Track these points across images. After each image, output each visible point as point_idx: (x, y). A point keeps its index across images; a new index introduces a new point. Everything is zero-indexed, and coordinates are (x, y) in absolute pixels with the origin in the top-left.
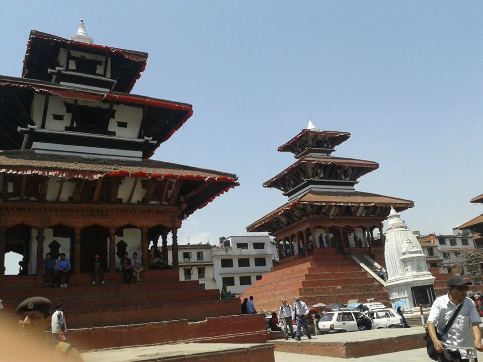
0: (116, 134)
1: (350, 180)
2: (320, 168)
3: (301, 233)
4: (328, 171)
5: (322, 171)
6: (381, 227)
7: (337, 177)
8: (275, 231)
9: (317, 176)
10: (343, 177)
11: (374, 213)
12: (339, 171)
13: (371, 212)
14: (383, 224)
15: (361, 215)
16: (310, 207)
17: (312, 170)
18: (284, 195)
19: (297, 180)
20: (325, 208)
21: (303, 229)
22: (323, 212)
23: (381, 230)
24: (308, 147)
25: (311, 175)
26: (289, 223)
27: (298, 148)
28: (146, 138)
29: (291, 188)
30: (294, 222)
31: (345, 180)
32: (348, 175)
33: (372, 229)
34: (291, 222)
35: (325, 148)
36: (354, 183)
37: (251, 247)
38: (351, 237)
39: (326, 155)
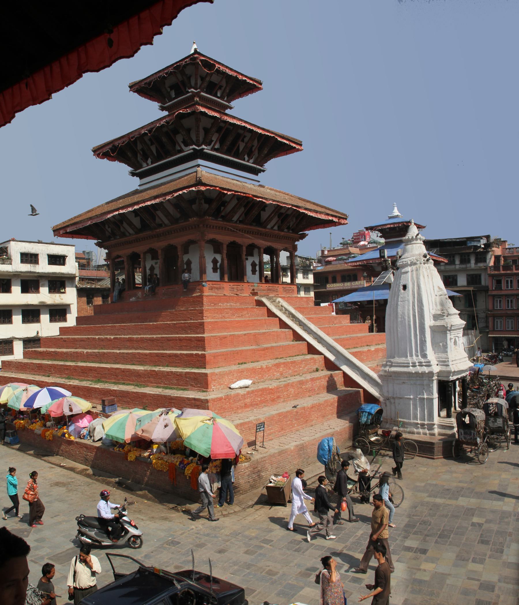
4: (230, 139)
9: (209, 145)
15: (272, 228)
18: (133, 174)
26: (145, 226)
27: (169, 90)
29: (149, 161)
30: (160, 226)
35: (218, 98)
36: (260, 171)
37: (43, 260)
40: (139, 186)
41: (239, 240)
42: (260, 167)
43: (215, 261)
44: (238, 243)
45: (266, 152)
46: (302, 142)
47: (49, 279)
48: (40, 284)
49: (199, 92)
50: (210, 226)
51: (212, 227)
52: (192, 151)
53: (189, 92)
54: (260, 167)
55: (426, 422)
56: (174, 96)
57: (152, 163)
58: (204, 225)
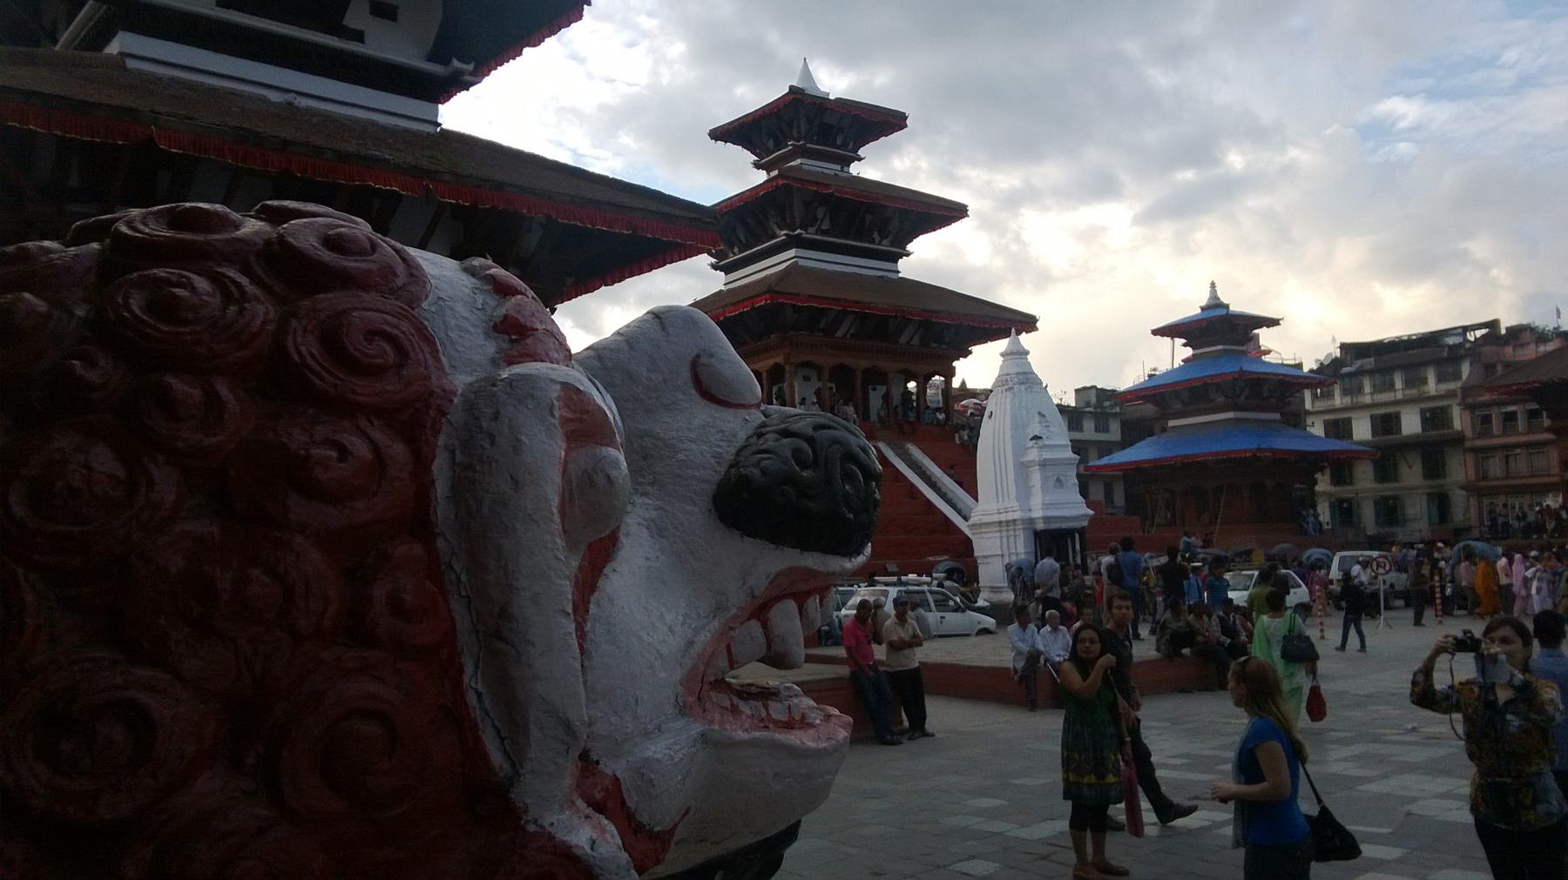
0: (367, 39)
6: (949, 373)
9: (812, 226)
10: (876, 235)
12: (869, 218)
14: (954, 368)
15: (908, 342)
18: (715, 267)
24: (795, 140)
25: (798, 224)
28: (456, 63)
29: (736, 250)
31: (880, 244)
32: (889, 232)
35: (838, 147)
39: (839, 167)
40: (725, 284)
41: (850, 361)
42: (900, 251)
52: (784, 237)
53: (788, 146)
54: (900, 251)
56: (772, 149)
57: (740, 253)
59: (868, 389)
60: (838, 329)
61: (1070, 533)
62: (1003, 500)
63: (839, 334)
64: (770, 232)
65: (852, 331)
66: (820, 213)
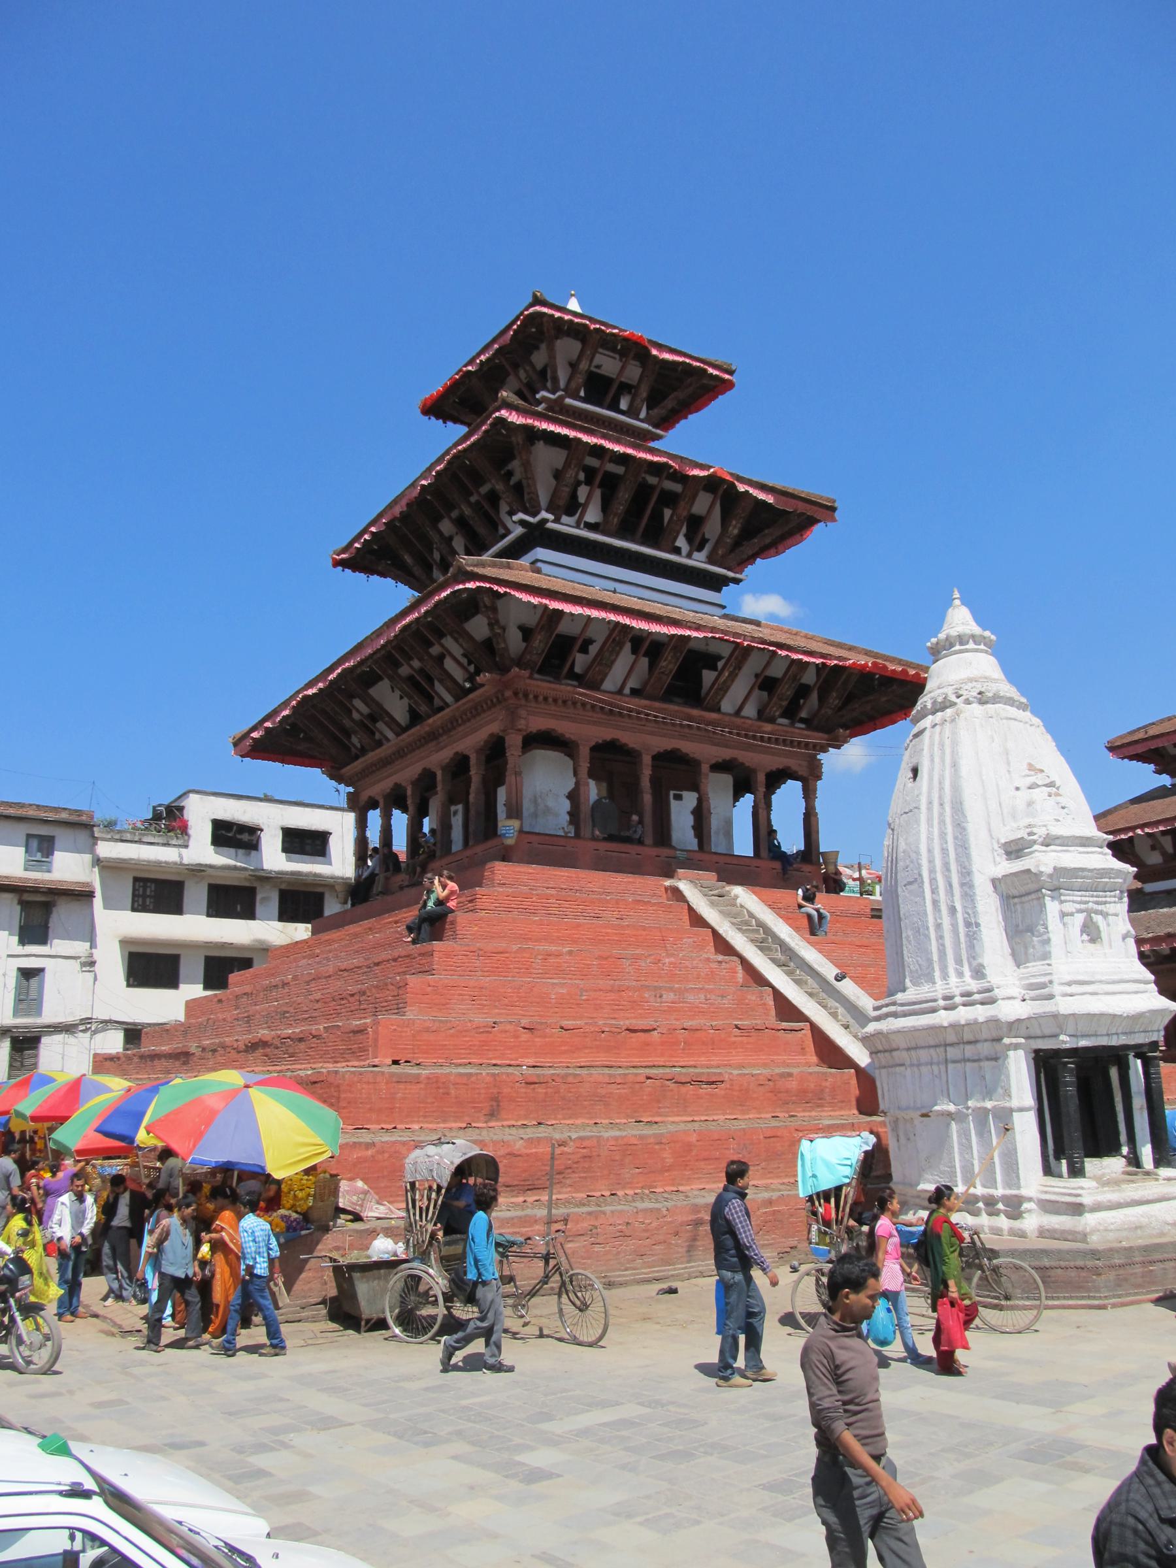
1: (711, 560)
2: (589, 481)
3: (460, 766)
4: (624, 495)
5: (598, 493)
6: (810, 777)
7: (656, 535)
8: (357, 758)
9: (570, 514)
11: (790, 713)
12: (667, 513)
13: (785, 703)
15: (738, 713)
16: (520, 635)
17: (554, 482)
19: (482, 530)
20: (584, 649)
21: (470, 741)
22: (578, 669)
23: (809, 794)
25: (544, 500)
26: (415, 718)
33: (776, 779)
34: (423, 709)
36: (726, 581)
38: (681, 812)
41: (629, 739)
43: (573, 796)
44: (626, 745)
45: (736, 531)
46: (834, 501)
47: (283, 887)
48: (259, 897)
49: (561, 398)
50: (536, 697)
51: (541, 698)
55: (999, 1192)
58: (516, 694)
59: (668, 795)
60: (605, 675)
61: (1117, 1056)
62: (945, 976)
63: (608, 685)
64: (502, 531)
65: (632, 683)
66: (583, 492)
